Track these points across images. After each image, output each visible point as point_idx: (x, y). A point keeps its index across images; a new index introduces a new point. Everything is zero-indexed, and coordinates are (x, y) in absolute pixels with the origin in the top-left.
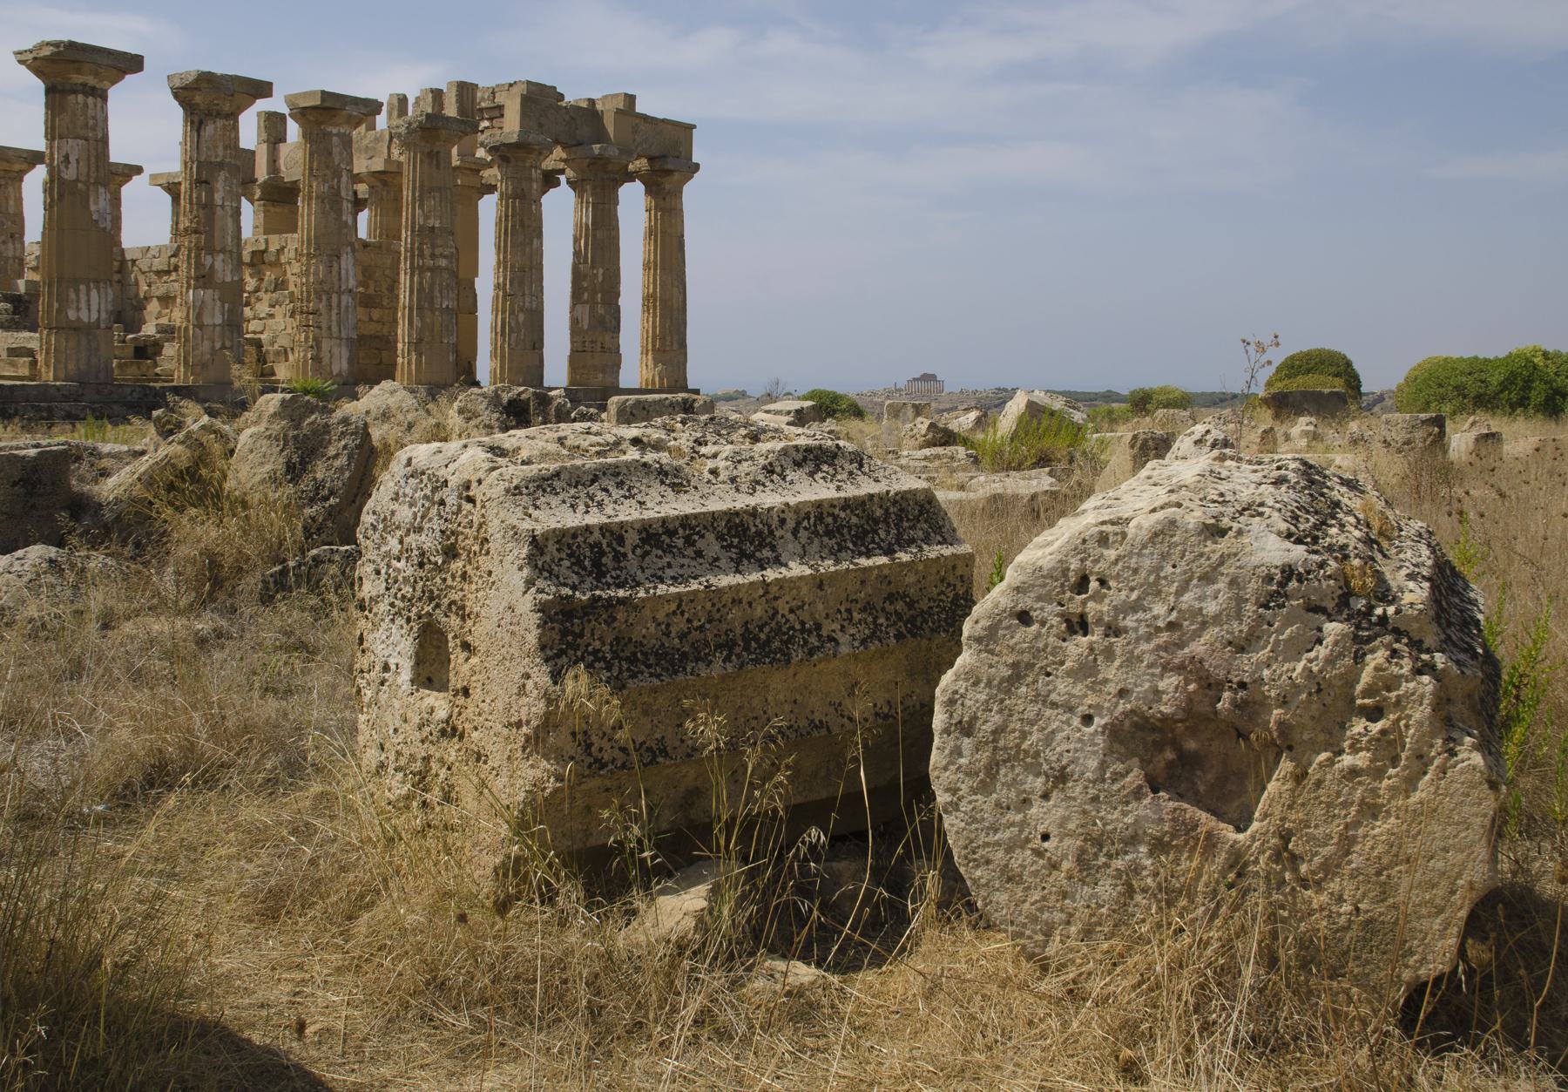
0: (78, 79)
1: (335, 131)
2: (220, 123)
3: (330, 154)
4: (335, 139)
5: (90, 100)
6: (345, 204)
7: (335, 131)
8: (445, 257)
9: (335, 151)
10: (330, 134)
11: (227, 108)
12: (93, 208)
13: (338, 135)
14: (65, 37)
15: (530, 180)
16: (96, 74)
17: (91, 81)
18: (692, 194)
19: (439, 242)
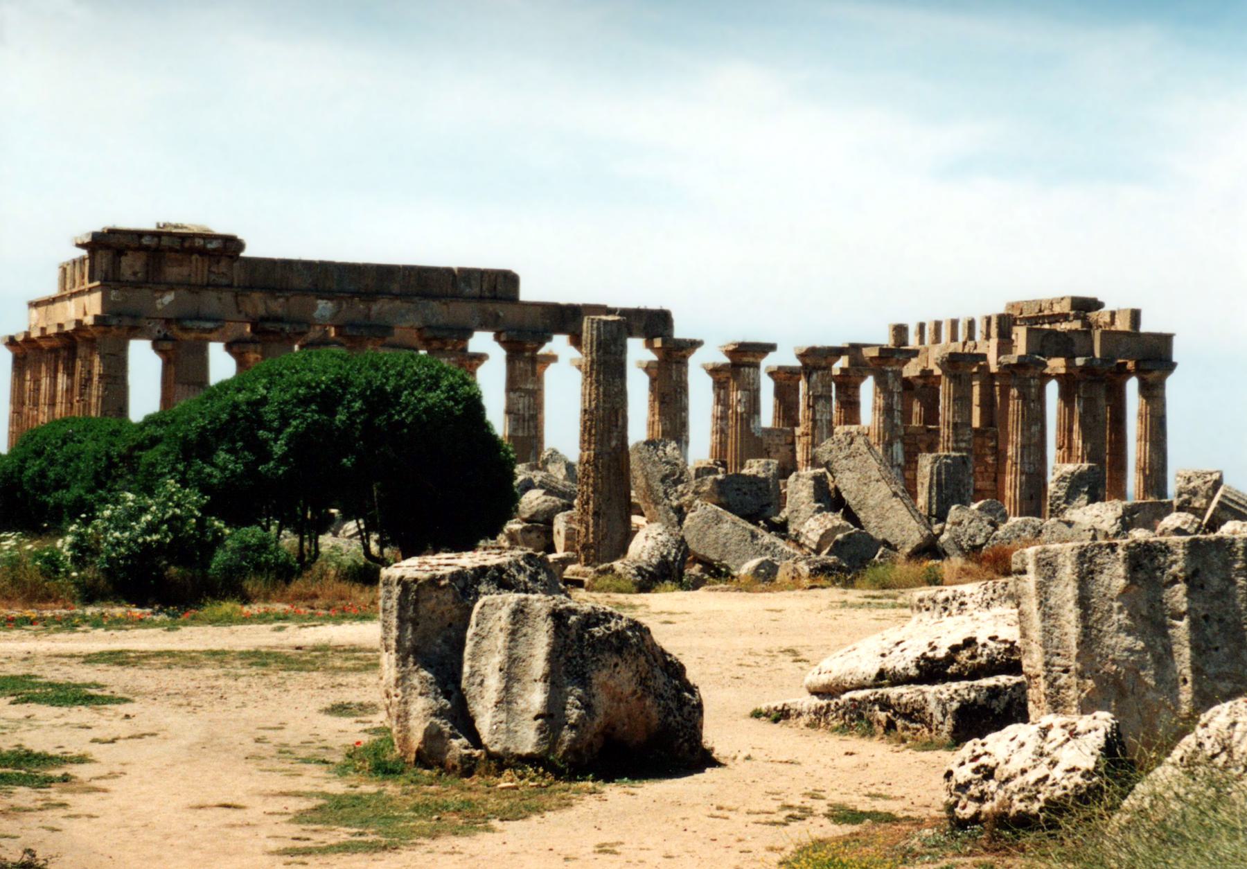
0: (745, 359)
1: (890, 369)
2: (820, 373)
3: (887, 383)
4: (890, 374)
5: (752, 370)
6: (896, 413)
7: (890, 369)
8: (965, 441)
9: (890, 381)
10: (887, 372)
11: (824, 364)
12: (752, 426)
13: (892, 371)
14: (740, 340)
15: (1030, 386)
16: (754, 356)
17: (751, 360)
18: (1173, 385)
19: (960, 432)
